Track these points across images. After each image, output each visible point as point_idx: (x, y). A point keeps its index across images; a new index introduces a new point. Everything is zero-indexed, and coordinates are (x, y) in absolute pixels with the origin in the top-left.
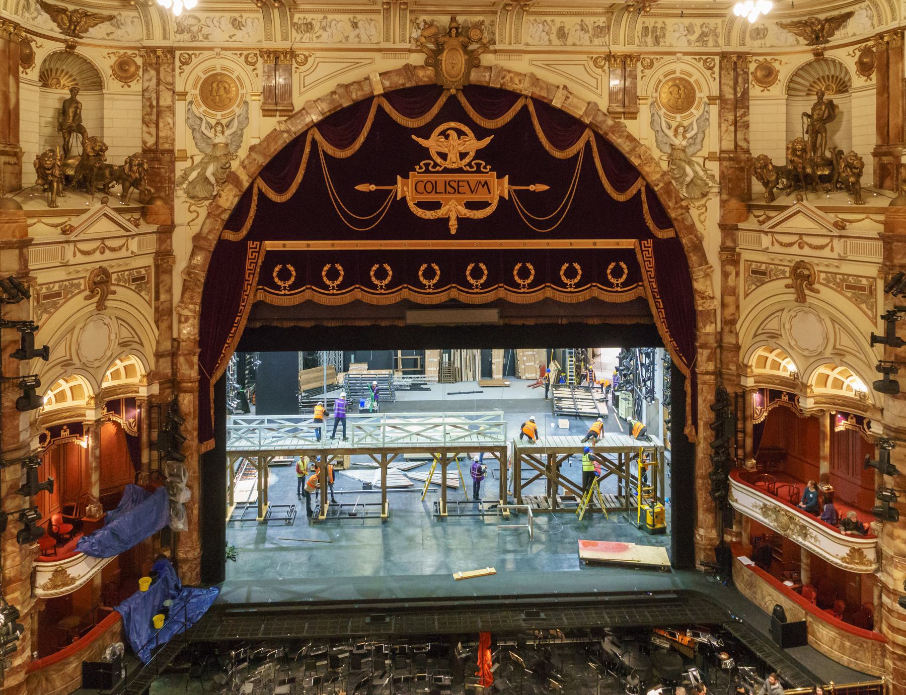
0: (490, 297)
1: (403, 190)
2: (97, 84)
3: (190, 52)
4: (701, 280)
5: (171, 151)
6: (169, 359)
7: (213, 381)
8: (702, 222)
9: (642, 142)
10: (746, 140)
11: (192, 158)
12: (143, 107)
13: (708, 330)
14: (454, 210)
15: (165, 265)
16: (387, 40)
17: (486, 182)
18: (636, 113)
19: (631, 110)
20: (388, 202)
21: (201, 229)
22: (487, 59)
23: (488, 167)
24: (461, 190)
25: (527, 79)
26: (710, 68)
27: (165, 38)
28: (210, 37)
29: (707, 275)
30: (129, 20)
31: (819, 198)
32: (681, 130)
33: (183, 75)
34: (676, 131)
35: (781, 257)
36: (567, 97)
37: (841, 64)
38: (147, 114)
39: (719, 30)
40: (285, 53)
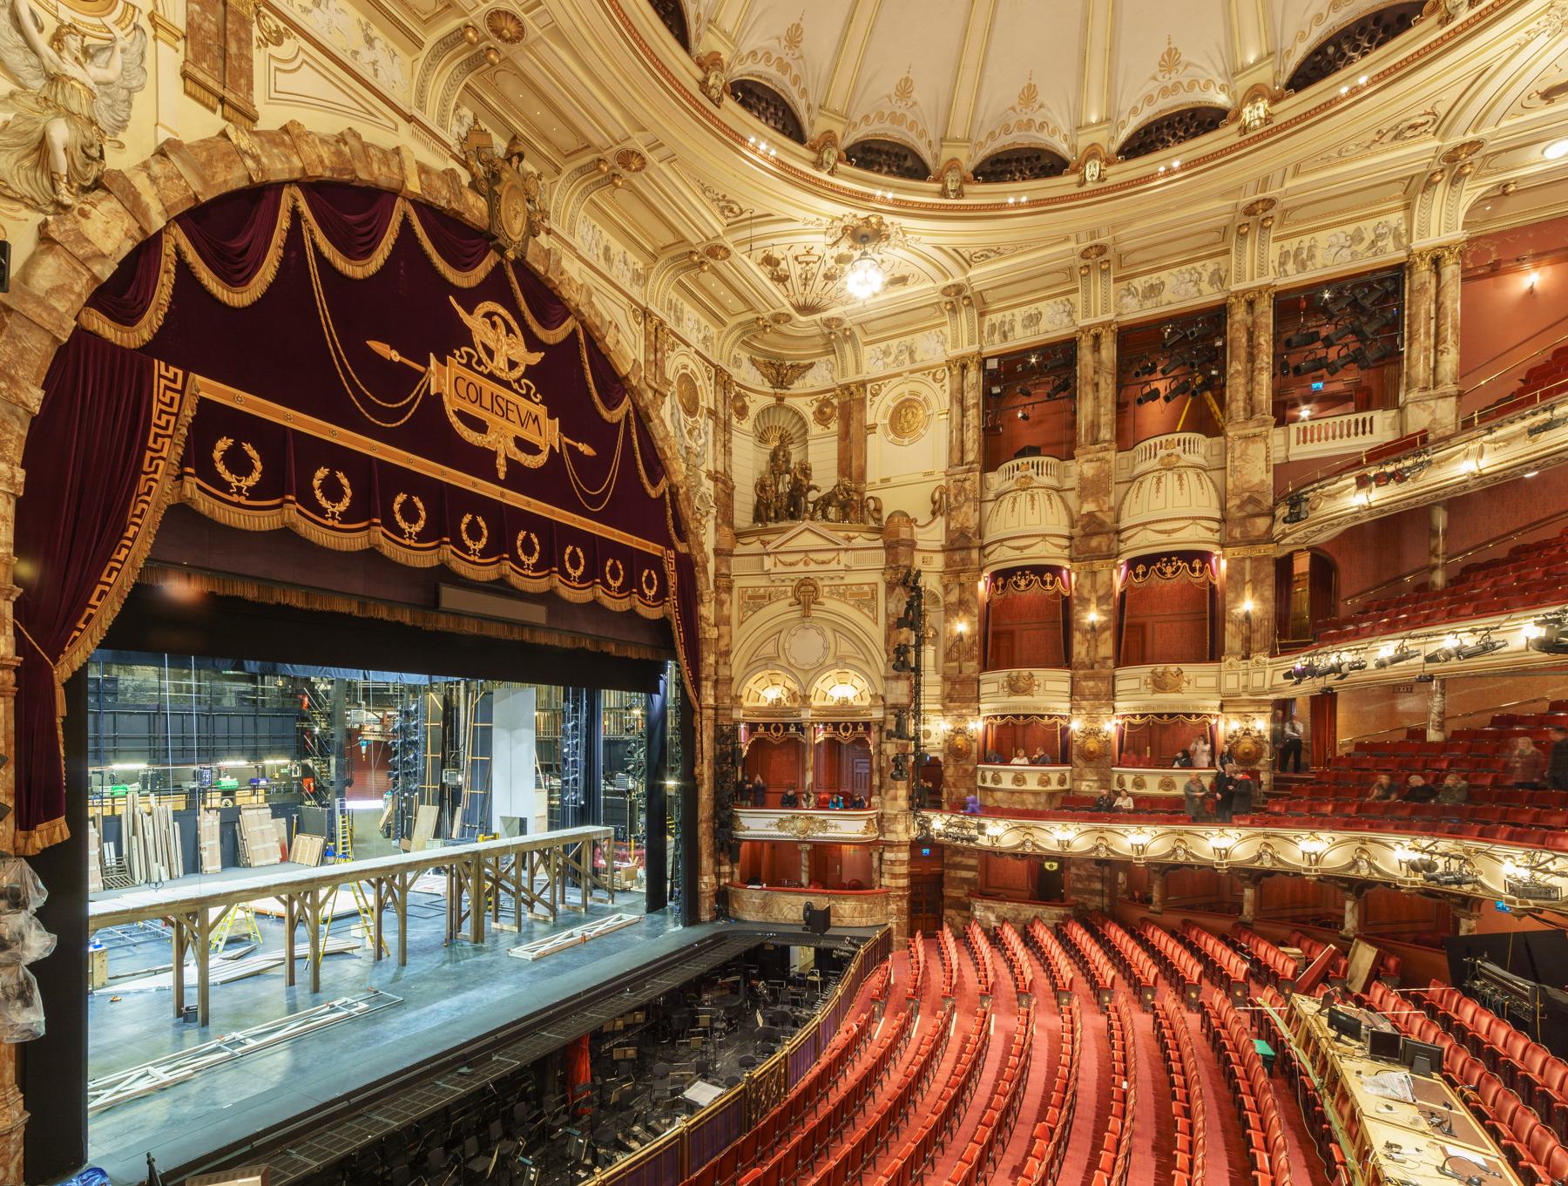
1: (438, 384)
20: (417, 393)
34: (690, 432)
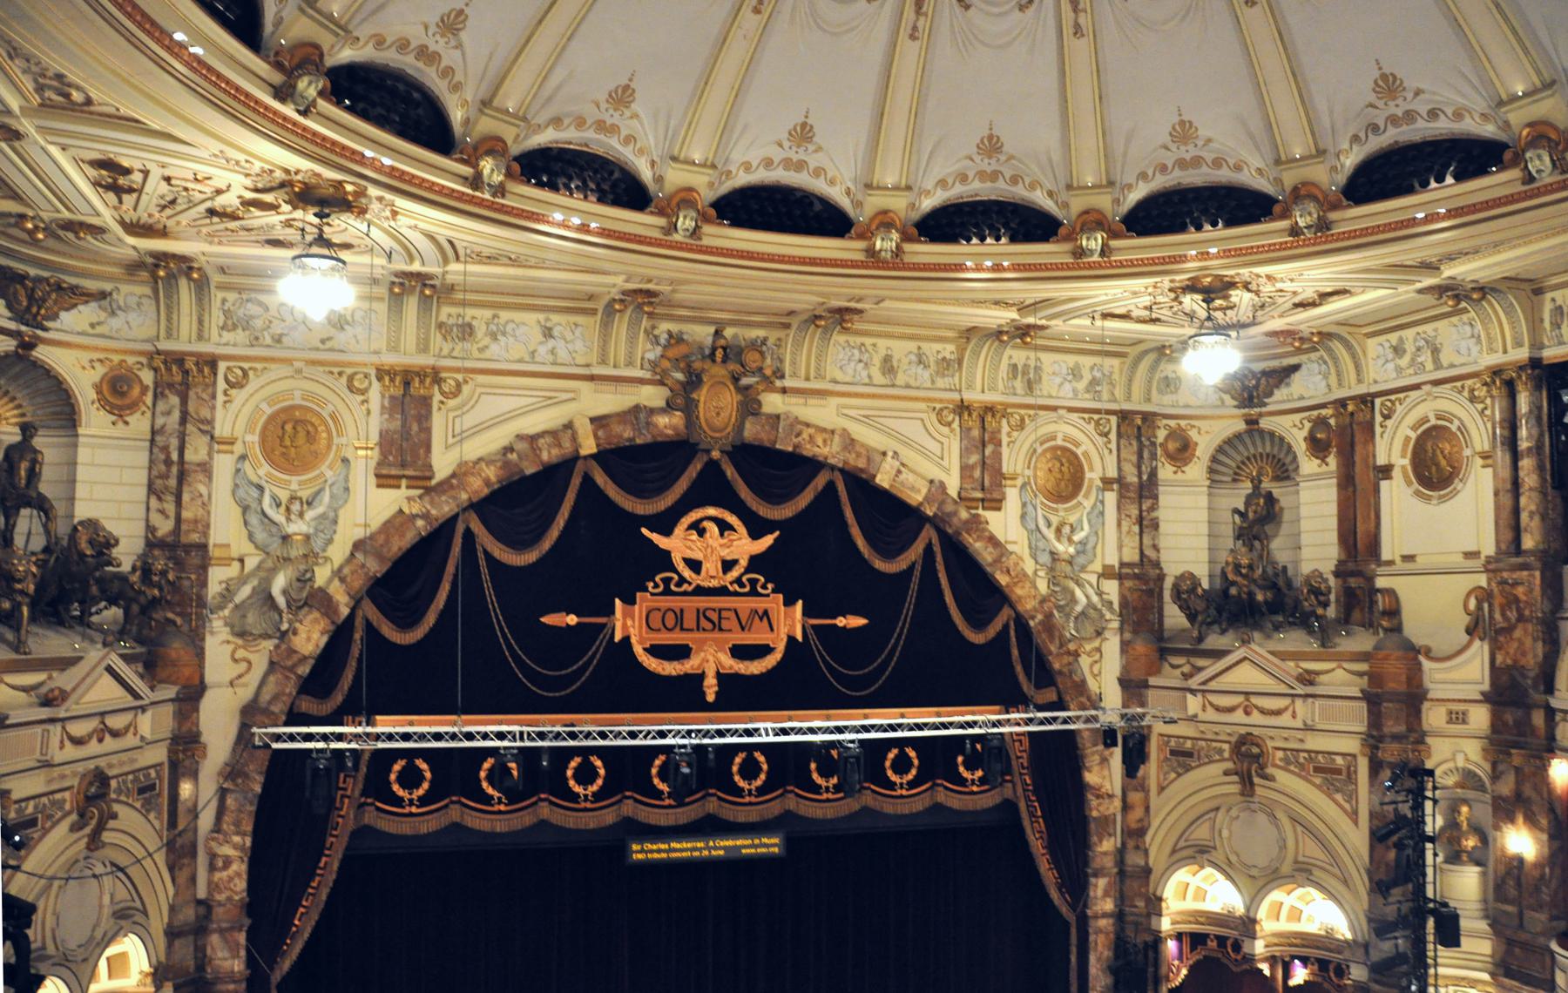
0: (774, 809)
1: (624, 626)
2: (66, 416)
3: (246, 365)
4: (1096, 769)
5: (203, 547)
8: (1095, 676)
9: (1010, 547)
10: (1155, 548)
11: (241, 561)
12: (151, 461)
13: (1106, 846)
14: (711, 659)
15: (187, 763)
16: (603, 361)
17: (766, 613)
18: (1000, 501)
19: (996, 495)
20: (599, 645)
22: (772, 402)
24: (725, 624)
25: (837, 438)
26: (1106, 435)
27: (200, 337)
28: (285, 339)
30: (133, 301)
31: (1269, 637)
32: (1066, 530)
33: (234, 407)
34: (1058, 531)
35: (1217, 728)
36: (899, 472)
37: (1282, 439)
38: (161, 477)
39: (1116, 376)
40: (421, 374)
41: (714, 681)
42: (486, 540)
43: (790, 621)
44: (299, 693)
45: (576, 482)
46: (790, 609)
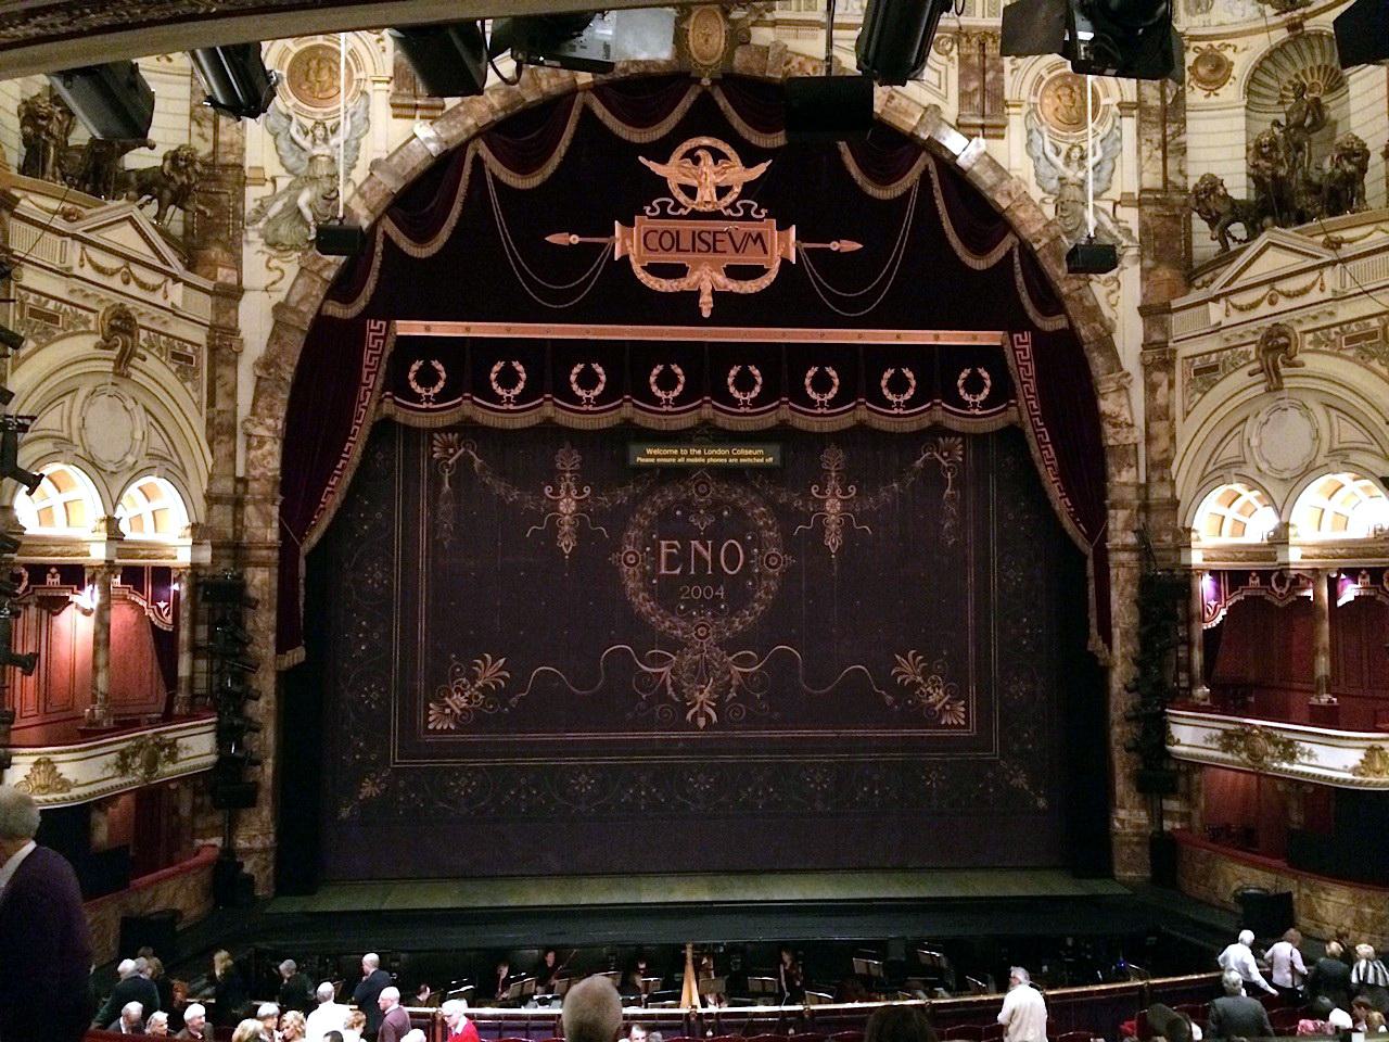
0: (769, 420)
1: (623, 244)
4: (1112, 396)
5: (241, 167)
6: (229, 508)
7: (305, 548)
9: (1012, 174)
11: (274, 181)
13: (1124, 479)
17: (759, 236)
18: (1003, 127)
19: (995, 121)
20: (599, 265)
21: (288, 295)
22: (763, 36)
23: (763, 211)
24: (719, 246)
29: (1122, 389)
41: (711, 299)
42: (493, 165)
43: (784, 245)
44: (326, 298)
45: (575, 113)
46: (783, 233)
